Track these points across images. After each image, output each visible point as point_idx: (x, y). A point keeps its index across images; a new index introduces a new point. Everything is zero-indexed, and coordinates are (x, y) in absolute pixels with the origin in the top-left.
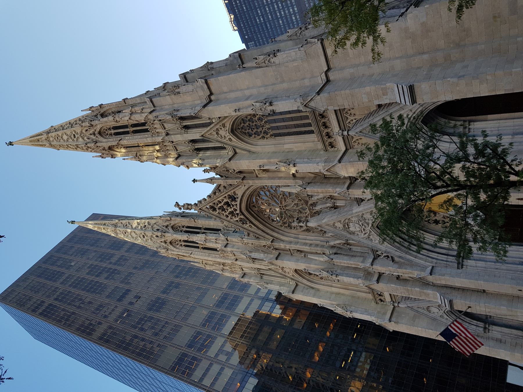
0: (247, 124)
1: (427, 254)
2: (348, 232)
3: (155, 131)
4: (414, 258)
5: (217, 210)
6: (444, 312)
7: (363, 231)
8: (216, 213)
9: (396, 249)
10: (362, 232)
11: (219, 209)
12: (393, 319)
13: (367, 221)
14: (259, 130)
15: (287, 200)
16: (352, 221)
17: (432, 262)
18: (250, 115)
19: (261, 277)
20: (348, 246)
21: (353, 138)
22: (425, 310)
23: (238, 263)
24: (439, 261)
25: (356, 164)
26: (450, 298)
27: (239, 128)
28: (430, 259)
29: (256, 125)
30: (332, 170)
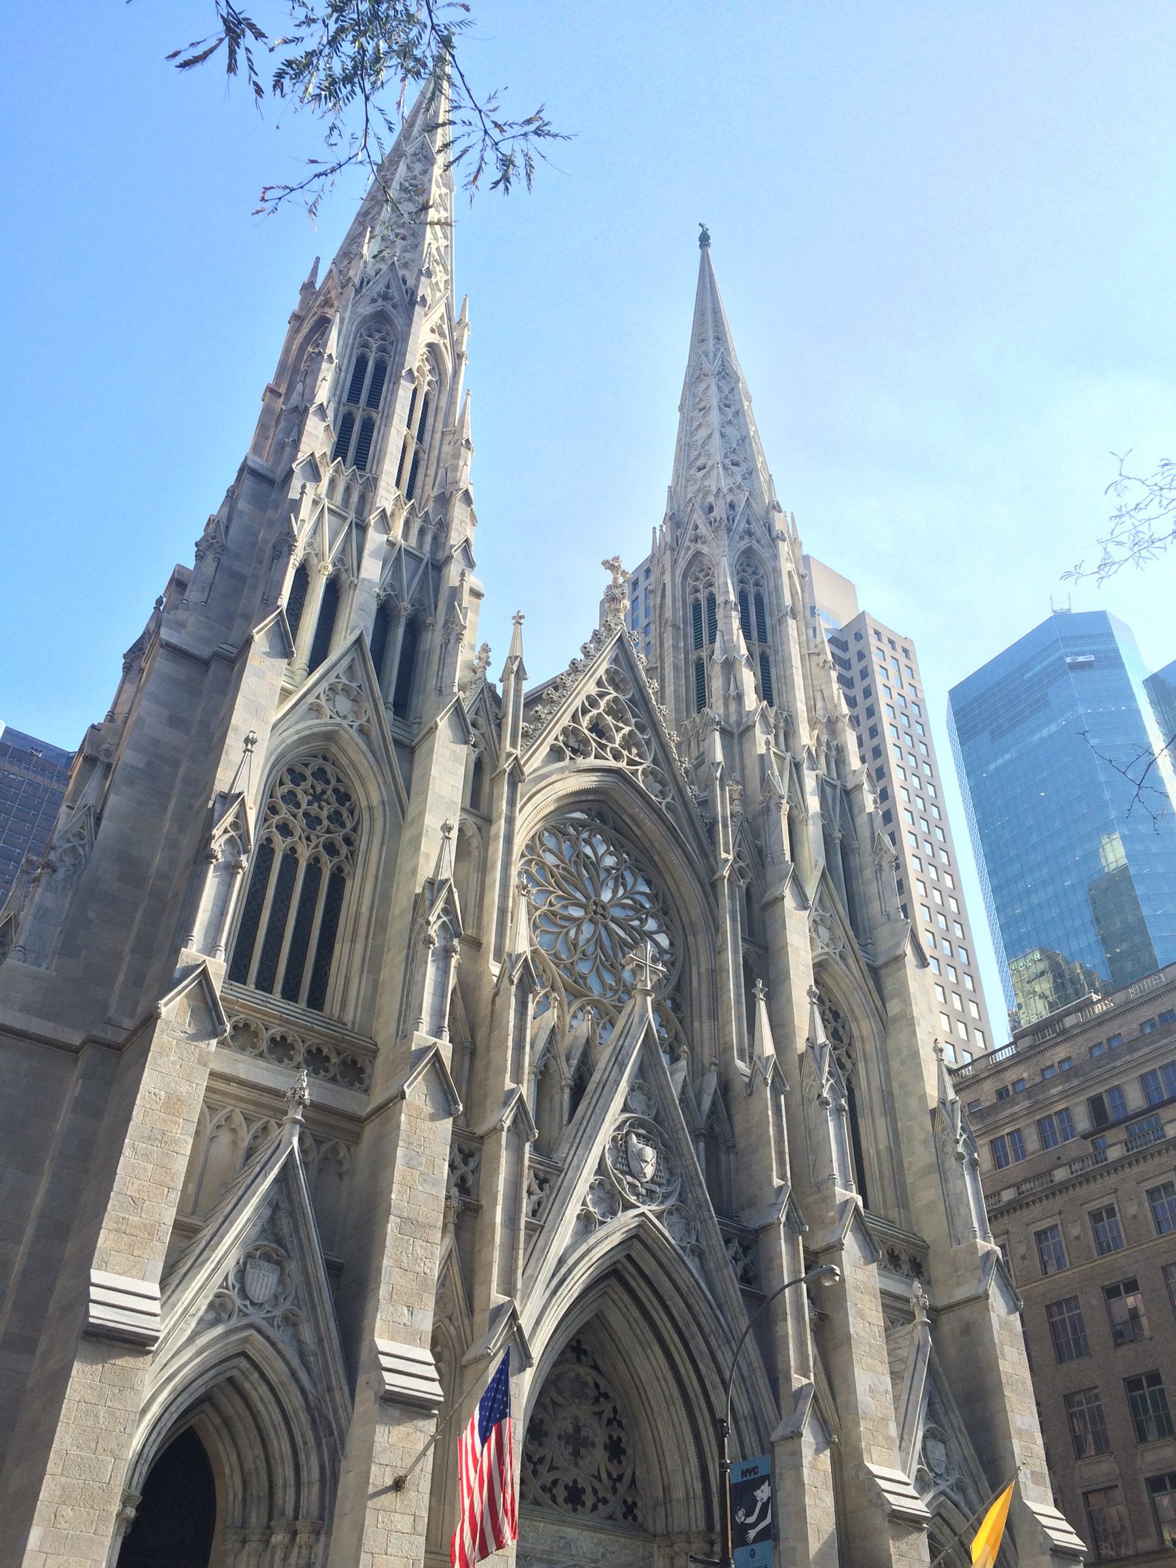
8: (601, 672)
11: (615, 700)
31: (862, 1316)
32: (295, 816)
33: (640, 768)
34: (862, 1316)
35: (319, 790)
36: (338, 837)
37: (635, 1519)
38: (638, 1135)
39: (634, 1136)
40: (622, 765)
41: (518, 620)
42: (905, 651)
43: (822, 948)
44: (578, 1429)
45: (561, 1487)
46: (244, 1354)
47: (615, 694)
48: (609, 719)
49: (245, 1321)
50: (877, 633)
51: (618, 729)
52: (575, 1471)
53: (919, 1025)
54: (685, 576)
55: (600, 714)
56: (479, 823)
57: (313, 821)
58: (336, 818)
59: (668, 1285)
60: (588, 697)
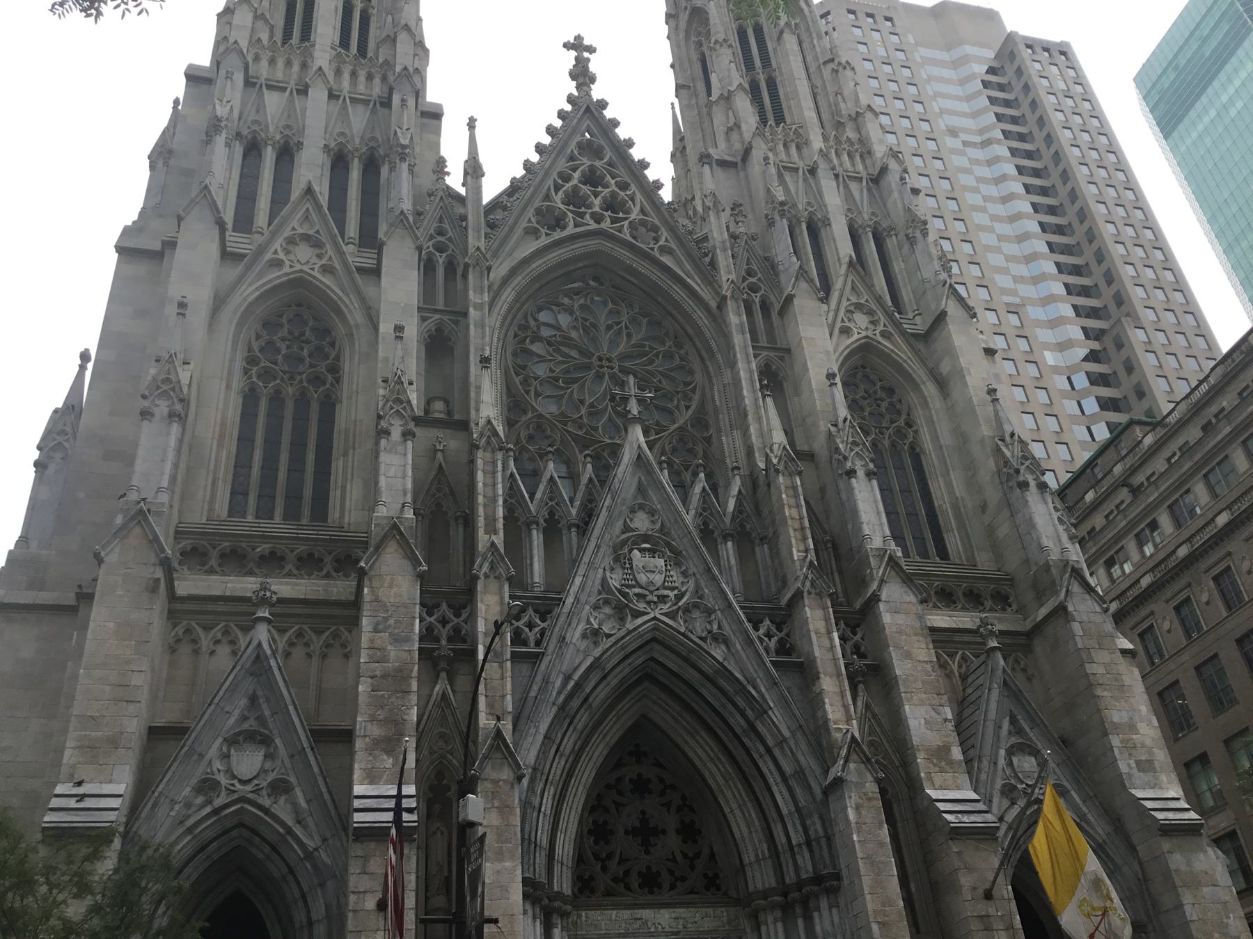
0: (880, 394)
1: (551, 777)
2: (624, 542)
3: (832, 147)
4: (543, 728)
5: (586, 162)
6: (242, 799)
7: (637, 590)
8: (572, 146)
9: (576, 677)
10: (628, 586)
11: (592, 169)
13: (680, 613)
14: (866, 414)
18: (908, 415)
23: (318, 95)
24: (535, 814)
25: (927, 644)
27: (864, 367)
30: (893, 573)
31: (908, 655)
32: (275, 363)
33: (626, 223)
34: (908, 655)
36: (322, 368)
37: (718, 888)
38: (642, 550)
39: (636, 552)
40: (606, 225)
41: (472, 124)
42: (1063, 53)
43: (859, 333)
46: (241, 825)
47: (589, 163)
48: (586, 189)
49: (235, 796)
50: (1029, 46)
51: (596, 195)
54: (687, 37)
56: (452, 318)
58: (318, 352)
59: (697, 675)
60: (560, 175)
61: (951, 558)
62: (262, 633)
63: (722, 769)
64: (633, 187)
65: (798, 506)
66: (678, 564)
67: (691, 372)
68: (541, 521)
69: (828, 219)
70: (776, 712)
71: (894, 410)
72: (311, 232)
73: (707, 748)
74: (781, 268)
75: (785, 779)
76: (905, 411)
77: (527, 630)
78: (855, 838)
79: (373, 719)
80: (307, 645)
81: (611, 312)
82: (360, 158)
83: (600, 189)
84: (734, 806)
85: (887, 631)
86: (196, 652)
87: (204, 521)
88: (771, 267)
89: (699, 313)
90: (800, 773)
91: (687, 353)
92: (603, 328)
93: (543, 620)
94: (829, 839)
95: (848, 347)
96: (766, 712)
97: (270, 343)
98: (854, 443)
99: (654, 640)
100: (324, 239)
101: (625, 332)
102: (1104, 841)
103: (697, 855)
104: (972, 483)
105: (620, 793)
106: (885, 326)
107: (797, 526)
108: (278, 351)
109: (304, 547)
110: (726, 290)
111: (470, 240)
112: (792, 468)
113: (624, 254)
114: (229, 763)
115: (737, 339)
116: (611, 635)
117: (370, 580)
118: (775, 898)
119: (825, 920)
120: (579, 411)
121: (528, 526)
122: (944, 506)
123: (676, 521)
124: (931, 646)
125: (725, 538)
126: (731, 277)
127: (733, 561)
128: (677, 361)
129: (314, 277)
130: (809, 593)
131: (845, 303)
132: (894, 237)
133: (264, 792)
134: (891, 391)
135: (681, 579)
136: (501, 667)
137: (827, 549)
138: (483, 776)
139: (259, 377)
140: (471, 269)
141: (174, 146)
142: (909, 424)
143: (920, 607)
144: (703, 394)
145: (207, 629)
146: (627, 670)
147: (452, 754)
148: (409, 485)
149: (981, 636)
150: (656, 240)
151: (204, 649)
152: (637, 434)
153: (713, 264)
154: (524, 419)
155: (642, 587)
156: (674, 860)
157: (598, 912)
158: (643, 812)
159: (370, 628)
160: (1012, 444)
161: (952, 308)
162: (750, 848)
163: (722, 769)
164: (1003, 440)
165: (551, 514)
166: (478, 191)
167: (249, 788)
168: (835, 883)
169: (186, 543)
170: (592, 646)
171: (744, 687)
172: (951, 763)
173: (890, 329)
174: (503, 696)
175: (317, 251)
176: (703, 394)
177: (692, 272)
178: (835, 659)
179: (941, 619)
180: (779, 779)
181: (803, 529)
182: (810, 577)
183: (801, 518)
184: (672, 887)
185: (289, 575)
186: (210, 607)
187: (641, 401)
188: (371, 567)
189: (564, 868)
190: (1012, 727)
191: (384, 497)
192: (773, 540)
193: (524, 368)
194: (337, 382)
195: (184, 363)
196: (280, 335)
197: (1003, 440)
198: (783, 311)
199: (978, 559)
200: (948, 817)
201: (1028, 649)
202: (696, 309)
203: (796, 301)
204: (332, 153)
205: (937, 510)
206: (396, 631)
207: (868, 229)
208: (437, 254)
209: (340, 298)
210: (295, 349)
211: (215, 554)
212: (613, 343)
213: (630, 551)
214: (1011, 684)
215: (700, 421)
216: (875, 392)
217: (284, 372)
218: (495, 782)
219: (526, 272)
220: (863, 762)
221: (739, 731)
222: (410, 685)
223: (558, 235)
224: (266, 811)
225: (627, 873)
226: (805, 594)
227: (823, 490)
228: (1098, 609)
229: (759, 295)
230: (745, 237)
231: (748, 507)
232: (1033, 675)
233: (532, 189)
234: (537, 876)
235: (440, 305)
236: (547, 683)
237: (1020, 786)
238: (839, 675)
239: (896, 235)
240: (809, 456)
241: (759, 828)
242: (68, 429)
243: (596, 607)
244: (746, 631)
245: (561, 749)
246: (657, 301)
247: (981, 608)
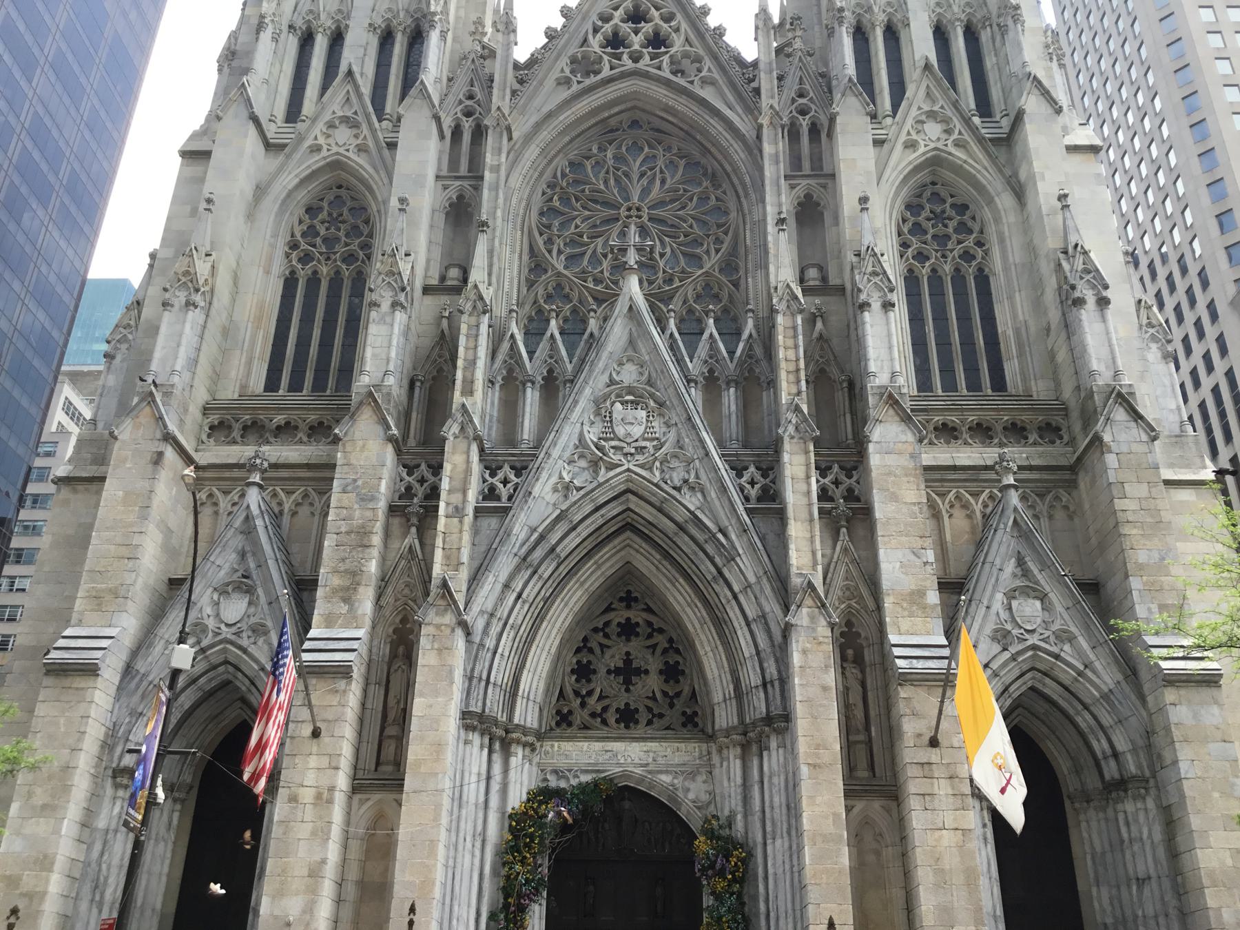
0: (950, 212)
1: (511, 621)
2: (606, 397)
4: (503, 577)
7: (613, 443)
9: (540, 530)
10: (605, 440)
12: (170, 453)
13: (657, 464)
14: (929, 236)
15: (667, 239)
16: (651, 418)
17: (486, 631)
18: (982, 232)
19: (295, 30)
20: (499, 378)
21: (942, 495)
22: (227, 574)
24: (489, 655)
25: (918, 485)
26: (356, 674)
27: (933, 183)
28: (495, 629)
29: (948, 237)
30: (891, 412)
32: (314, 246)
33: (666, 59)
34: (894, 498)
35: (335, 215)
36: (354, 246)
37: (696, 725)
39: (618, 405)
43: (926, 146)
44: (628, 661)
45: (612, 710)
46: (226, 662)
48: (626, 28)
51: (636, 32)
52: (626, 695)
53: (1043, 178)
55: (616, 24)
57: (329, 242)
61: (1009, 389)
62: (254, 497)
63: (699, 614)
64: (679, 17)
65: (796, 347)
66: (660, 415)
67: (726, 213)
68: (540, 379)
69: (908, 19)
70: (744, 559)
71: (963, 228)
72: (349, 114)
73: (685, 594)
74: (834, 83)
75: (748, 625)
76: (976, 228)
77: (502, 485)
78: (797, 681)
79: (335, 571)
80: (311, 504)
81: (647, 157)
82: (404, 32)
83: (643, 24)
84: (708, 649)
85: (874, 474)
86: (216, 513)
87: (236, 397)
88: (826, 83)
89: (735, 146)
90: (764, 616)
91: (724, 193)
92: (635, 177)
93: (517, 476)
94: (784, 680)
95: (910, 163)
96: (733, 559)
97: (312, 227)
98: (875, 274)
99: (628, 491)
100: (360, 118)
101: (658, 176)
102: (1110, 690)
103: (678, 694)
104: (1037, 304)
105: (606, 636)
106: (960, 133)
107: (792, 367)
108: (318, 234)
109: (313, 417)
110: (764, 121)
111: (494, 99)
112: (794, 306)
113: (660, 93)
114: (218, 609)
115: (769, 171)
116: (582, 488)
117: (344, 445)
118: (734, 736)
119: (774, 759)
120: (601, 264)
121: (524, 385)
122: (1008, 332)
123: (662, 372)
124: (923, 486)
125: (728, 384)
126: (771, 101)
127: (733, 408)
128: (713, 201)
129: (349, 158)
130: (792, 438)
131: (914, 112)
132: (988, 28)
133: (244, 635)
134: (962, 208)
135: (664, 429)
136: (461, 522)
137: (842, 389)
138: (426, 621)
139: (300, 260)
140: (490, 132)
141: (237, 48)
142: (980, 244)
143: (917, 447)
144: (736, 236)
145: (226, 493)
146: (600, 522)
147: (415, 601)
148: (393, 354)
149: (997, 473)
150: (699, 70)
151: (221, 511)
152: (633, 287)
153: (757, 91)
154: (544, 277)
155: (620, 440)
156: (654, 698)
157: (571, 743)
158: (628, 654)
159: (339, 489)
160: (1074, 257)
161: (1032, 104)
162: (719, 688)
163: (699, 614)
164: (1065, 252)
165: (550, 371)
166: (509, 45)
167: (234, 629)
168: (783, 724)
169: (214, 418)
170: (561, 499)
171: (714, 536)
172: (924, 607)
173: (966, 137)
174: (459, 549)
175: (355, 131)
176: (736, 236)
177: (735, 103)
178: (810, 505)
179: (968, 455)
180: (743, 623)
181: (798, 370)
182: (794, 421)
183: (797, 360)
184: (650, 723)
185: (301, 442)
186: (227, 474)
187: (640, 250)
188: (346, 433)
189: (531, 703)
190: (1019, 569)
191: (368, 367)
192: (773, 384)
193: (549, 227)
194: (369, 258)
195: (207, 255)
196: (320, 217)
197: (1065, 252)
198: (830, 135)
199: (1034, 389)
200: (900, 663)
201: (1072, 485)
202: (732, 142)
203: (839, 120)
204: (379, 31)
205: (1000, 335)
206: (363, 491)
207: (957, 23)
208: (464, 119)
209: (371, 176)
210: (333, 230)
211: (237, 427)
212: (645, 191)
213: (613, 404)
214: (1022, 524)
215: (730, 266)
216: (943, 212)
217: (321, 254)
218: (438, 627)
219: (552, 127)
220: (818, 607)
221: (709, 577)
222: (370, 540)
223: (593, 79)
224: (245, 651)
225: (605, 709)
226: (786, 439)
227: (848, 326)
228: (1144, 437)
229: (807, 117)
230: (800, 53)
231: (758, 351)
232: (1074, 512)
233: (567, 36)
234: (487, 710)
235: (463, 169)
236: (509, 535)
237: (1015, 632)
238: (811, 520)
239: (991, 26)
240: (841, 290)
241: (727, 669)
242: (132, 323)
243: (570, 462)
244: (720, 480)
245: (524, 596)
246: (696, 139)
247: (1023, 441)
